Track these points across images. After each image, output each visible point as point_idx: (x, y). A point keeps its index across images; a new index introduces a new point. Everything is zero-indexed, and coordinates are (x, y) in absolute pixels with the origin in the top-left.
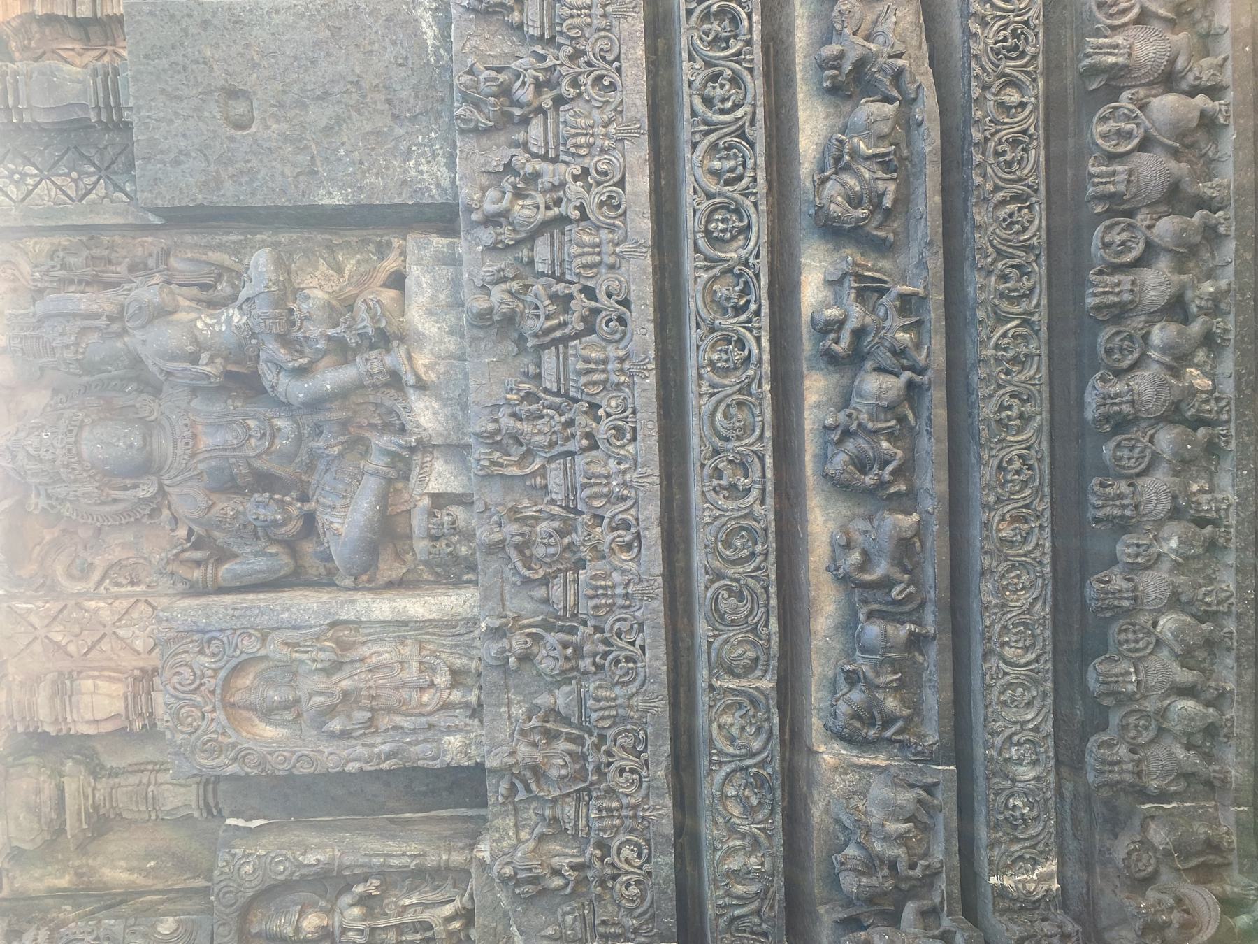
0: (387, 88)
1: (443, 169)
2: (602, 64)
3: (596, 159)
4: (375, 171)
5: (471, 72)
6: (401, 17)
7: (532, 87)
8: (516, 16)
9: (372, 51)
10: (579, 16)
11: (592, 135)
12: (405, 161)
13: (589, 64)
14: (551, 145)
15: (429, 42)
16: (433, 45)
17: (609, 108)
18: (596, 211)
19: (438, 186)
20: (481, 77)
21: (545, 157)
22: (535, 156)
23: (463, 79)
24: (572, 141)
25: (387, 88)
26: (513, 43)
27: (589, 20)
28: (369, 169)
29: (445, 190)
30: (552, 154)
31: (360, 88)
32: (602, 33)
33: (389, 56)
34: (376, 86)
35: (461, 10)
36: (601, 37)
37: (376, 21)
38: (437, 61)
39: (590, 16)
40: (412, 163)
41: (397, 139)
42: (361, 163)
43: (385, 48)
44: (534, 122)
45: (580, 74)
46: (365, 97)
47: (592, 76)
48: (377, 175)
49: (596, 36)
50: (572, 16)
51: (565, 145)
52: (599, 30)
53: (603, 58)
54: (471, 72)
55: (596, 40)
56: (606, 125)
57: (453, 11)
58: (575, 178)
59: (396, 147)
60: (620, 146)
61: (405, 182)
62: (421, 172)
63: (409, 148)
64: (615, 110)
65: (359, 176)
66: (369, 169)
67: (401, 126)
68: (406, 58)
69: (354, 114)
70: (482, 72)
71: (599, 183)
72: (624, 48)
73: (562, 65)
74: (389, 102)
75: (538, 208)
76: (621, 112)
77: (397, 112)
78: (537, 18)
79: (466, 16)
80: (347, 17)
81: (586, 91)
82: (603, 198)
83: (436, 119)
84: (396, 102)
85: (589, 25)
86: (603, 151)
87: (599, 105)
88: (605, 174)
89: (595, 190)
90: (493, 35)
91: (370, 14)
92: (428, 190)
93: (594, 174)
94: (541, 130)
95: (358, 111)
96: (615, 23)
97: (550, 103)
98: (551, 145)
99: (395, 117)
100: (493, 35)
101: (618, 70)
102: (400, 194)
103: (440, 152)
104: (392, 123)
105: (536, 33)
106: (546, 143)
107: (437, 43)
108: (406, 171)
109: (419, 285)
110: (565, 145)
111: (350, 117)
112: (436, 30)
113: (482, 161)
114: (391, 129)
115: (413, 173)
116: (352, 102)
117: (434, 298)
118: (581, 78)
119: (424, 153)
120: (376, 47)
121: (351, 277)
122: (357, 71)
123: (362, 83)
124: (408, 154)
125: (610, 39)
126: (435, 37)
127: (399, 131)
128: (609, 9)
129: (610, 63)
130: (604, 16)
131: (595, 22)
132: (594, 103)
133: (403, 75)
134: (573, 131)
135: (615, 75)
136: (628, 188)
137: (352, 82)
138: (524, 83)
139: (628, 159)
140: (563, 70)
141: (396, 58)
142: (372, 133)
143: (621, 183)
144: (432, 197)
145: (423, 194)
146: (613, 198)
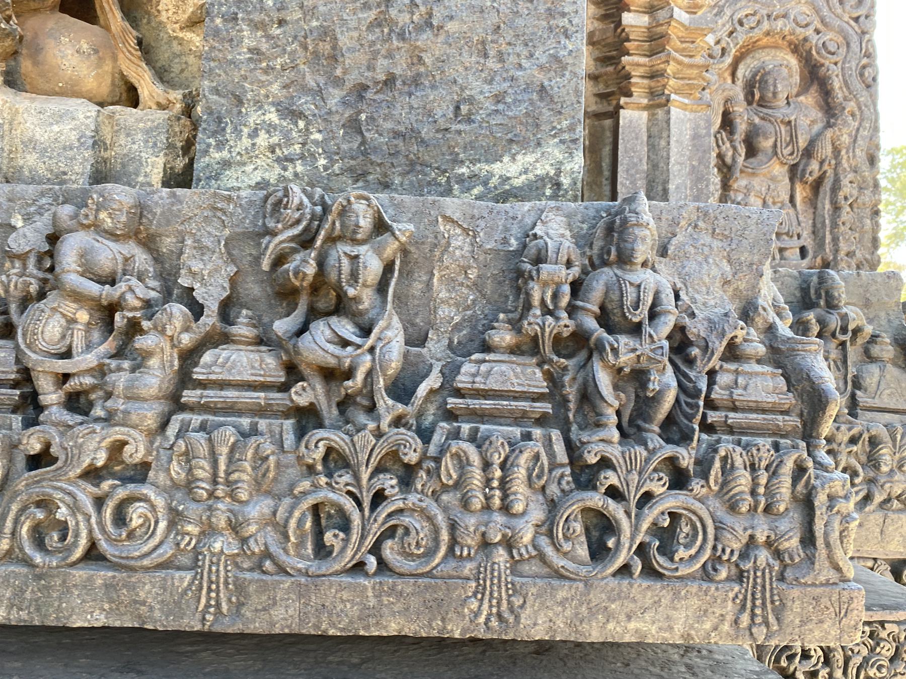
0: (416, 81)
1: (257, 177)
2: (375, 530)
3: (160, 502)
4: (264, 47)
5: (381, 227)
6: (546, 114)
7: (332, 362)
8: (503, 336)
9: (486, 56)
10: (488, 482)
11: (211, 495)
12: (277, 104)
13: (379, 498)
14: (212, 396)
15: (497, 168)
16: (491, 174)
17: (271, 537)
18: (36, 492)
19: (226, 164)
20: (362, 249)
21: (184, 379)
22: (190, 357)
23: (360, 207)
24: (203, 449)
25: (416, 81)
26: (457, 328)
27: (477, 503)
28: (269, 37)
29: (217, 177)
30: (190, 396)
31: (419, 29)
32: (445, 536)
33: (476, 87)
34: (420, 59)
35: (529, 221)
36: (436, 531)
37: (541, 67)
38: (460, 180)
39: (487, 507)
40: (273, 117)
41: (319, 93)
42: (281, 23)
43: (490, 82)
44: (271, 361)
45: (357, 477)
46: (402, 36)
47: (349, 504)
48: (253, 50)
49: (440, 519)
50: (487, 465)
51: (203, 427)
52: (453, 527)
53: (390, 533)
54: (381, 227)
55: (430, 519)
56: (235, 527)
57: (527, 206)
58: (118, 447)
59: (305, 90)
60: (185, 560)
61: (240, 102)
62: (254, 134)
63: (301, 115)
64: (267, 554)
65: (256, 17)
66: (269, 37)
67: (344, 103)
68: (469, 121)
69: (372, 15)
70: (379, 252)
71: (99, 502)
72: (405, 586)
73: (379, 434)
74: (390, 81)
75: (67, 354)
76: (259, 567)
77: (369, 95)
78: (493, 384)
79: (515, 230)
80: (550, 14)
81: (316, 487)
82: (62, 513)
83: (351, 170)
84: (386, 96)
85: (465, 504)
86: (176, 518)
87: (281, 514)
88: (120, 519)
89: (85, 494)
90: (477, 286)
91: (556, 58)
92: (220, 146)
93: (122, 493)
94: (247, 377)
95: (377, 23)
96: (468, 568)
97: (303, 401)
98: (212, 396)
99: (361, 89)
100: (477, 286)
101: (359, 567)
102: (216, 91)
103: (289, 174)
104: (349, 85)
105: (463, 380)
106: (223, 385)
107: (494, 181)
108: (259, 104)
109: (59, 118)
110: (203, 427)
111: (366, 6)
112: (517, 182)
113: (207, 242)
114: (338, 82)
115: (254, 118)
116: (393, 12)
117: (30, 144)
118: (347, 478)
119: (289, 142)
120: (492, 64)
121: (181, 41)
122: (451, 26)
123: (427, 34)
124: (292, 113)
125: (430, 553)
126: (505, 179)
127: (335, 97)
128: (501, 556)
129: (376, 550)
130: (486, 544)
131: (471, 521)
132: (287, 501)
133: (439, 113)
134: (224, 451)
135: (347, 559)
136: (80, 574)
137: (430, 15)
138: (345, 343)
139: (146, 578)
140: (365, 439)
141: (471, 100)
142: (334, 48)
143: (93, 555)
144: (206, 152)
145: (214, 134)
146: (63, 538)
